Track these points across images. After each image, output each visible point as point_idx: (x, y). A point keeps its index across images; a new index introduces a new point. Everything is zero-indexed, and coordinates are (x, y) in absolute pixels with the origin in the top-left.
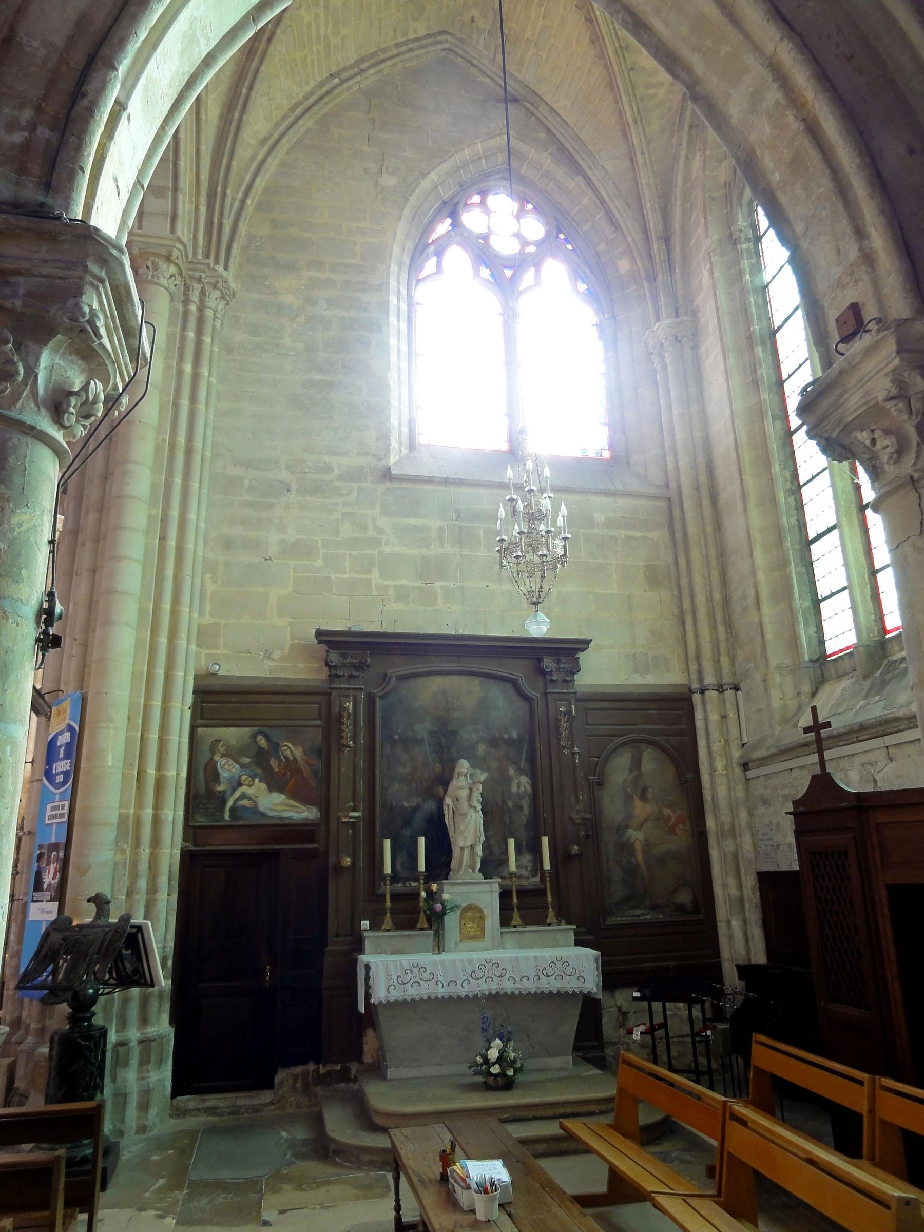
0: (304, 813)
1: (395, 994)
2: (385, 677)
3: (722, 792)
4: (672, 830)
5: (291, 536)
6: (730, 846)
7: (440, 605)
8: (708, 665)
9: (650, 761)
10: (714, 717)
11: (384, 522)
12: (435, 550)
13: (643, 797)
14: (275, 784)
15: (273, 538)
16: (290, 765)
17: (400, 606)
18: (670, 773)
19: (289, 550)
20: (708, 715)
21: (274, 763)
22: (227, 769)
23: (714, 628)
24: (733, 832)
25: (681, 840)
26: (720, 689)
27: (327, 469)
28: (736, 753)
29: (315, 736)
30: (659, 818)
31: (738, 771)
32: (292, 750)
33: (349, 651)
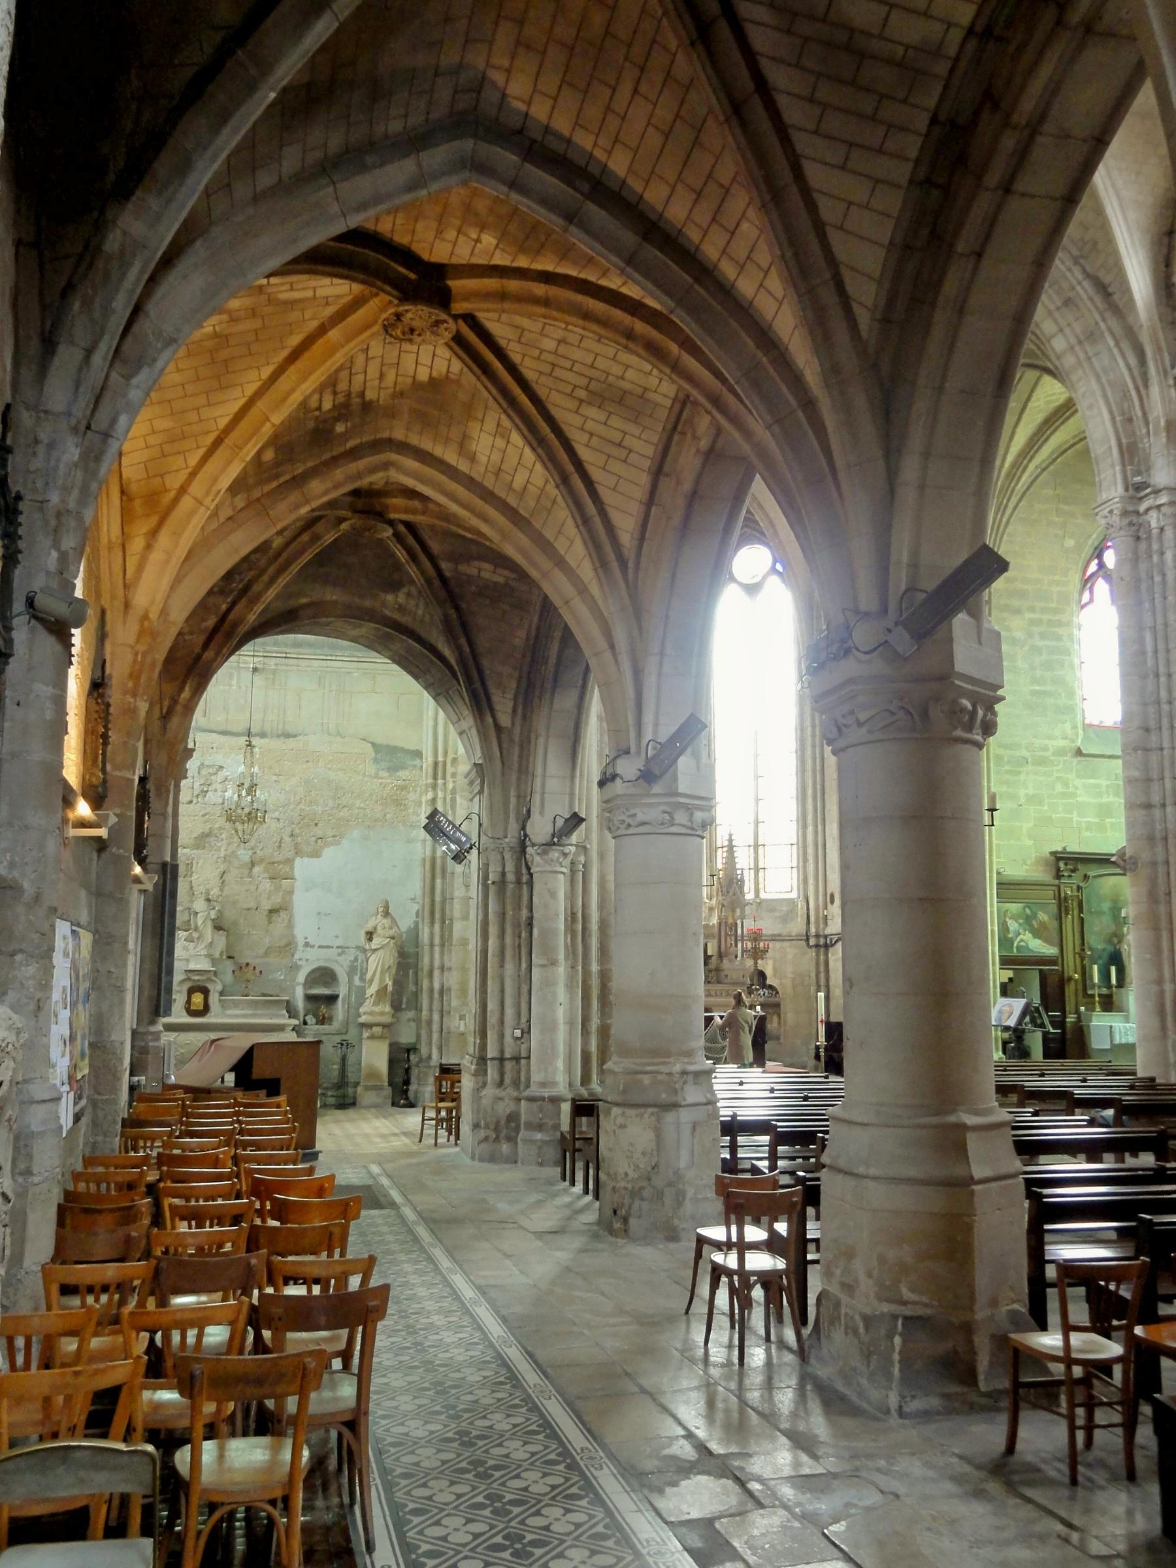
0: (1051, 951)
1: (1124, 1041)
2: (1086, 877)
5: (1031, 791)
7: (1109, 833)
11: (1078, 782)
12: (1105, 800)
14: (1037, 934)
15: (1022, 792)
16: (1042, 924)
17: (1088, 834)
19: (1034, 799)
21: (1034, 923)
22: (1013, 926)
27: (1046, 749)
29: (1054, 909)
32: (1043, 916)
33: (1060, 858)
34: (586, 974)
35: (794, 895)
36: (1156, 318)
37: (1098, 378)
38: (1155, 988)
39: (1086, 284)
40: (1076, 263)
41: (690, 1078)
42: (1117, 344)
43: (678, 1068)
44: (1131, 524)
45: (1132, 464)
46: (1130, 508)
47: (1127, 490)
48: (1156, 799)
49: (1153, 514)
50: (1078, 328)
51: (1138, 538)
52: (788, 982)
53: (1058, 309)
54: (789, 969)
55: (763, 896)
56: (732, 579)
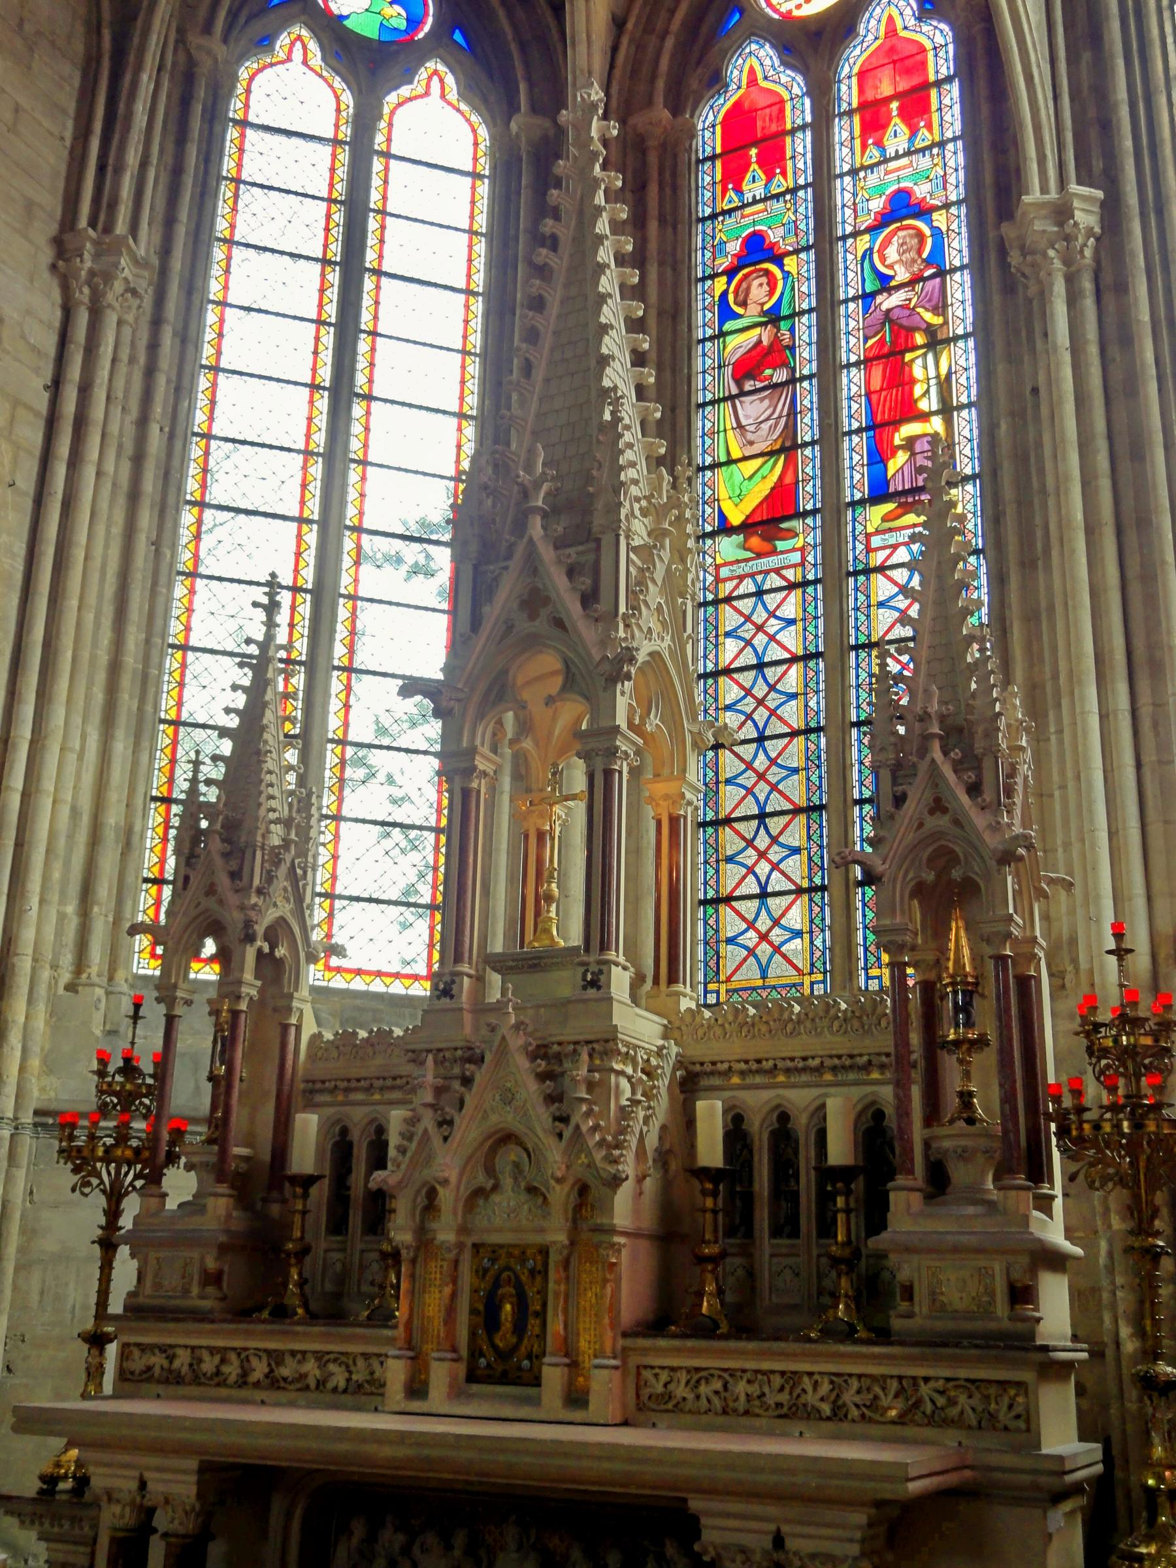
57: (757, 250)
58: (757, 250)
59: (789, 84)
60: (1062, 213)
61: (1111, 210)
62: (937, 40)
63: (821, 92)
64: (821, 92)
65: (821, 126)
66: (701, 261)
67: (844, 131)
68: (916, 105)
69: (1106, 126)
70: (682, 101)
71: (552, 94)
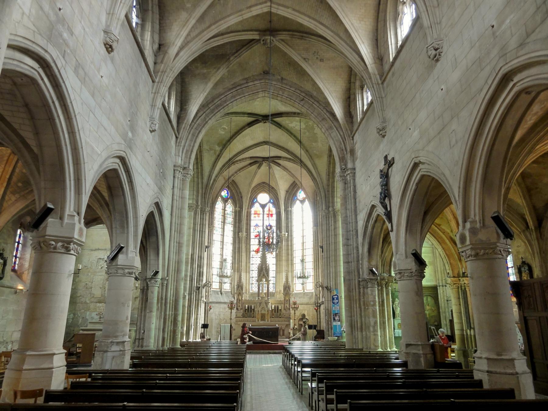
3: (443, 305)
4: (433, 311)
6: (444, 315)
8: (440, 281)
9: (429, 299)
10: (442, 291)
13: (428, 305)
18: (433, 301)
20: (440, 291)
23: (441, 274)
24: (445, 312)
25: (435, 313)
26: (443, 286)
28: (446, 298)
30: (431, 309)
31: (446, 302)
34: (165, 315)
35: (313, 291)
36: (345, 122)
37: (333, 140)
38: (349, 318)
39: (327, 114)
40: (324, 108)
41: (115, 344)
42: (337, 130)
43: (110, 341)
44: (343, 179)
45: (343, 162)
46: (342, 175)
47: (341, 170)
48: (350, 260)
49: (348, 176)
50: (326, 125)
51: (346, 183)
52: (311, 317)
53: (320, 121)
54: (311, 313)
55: (306, 291)
56: (297, 199)
57: (257, 226)
58: (257, 226)
59: (261, 210)
60: (285, 235)
61: (288, 235)
62: (274, 211)
63: (264, 212)
64: (264, 212)
65: (263, 215)
66: (252, 225)
67: (265, 216)
68: (272, 215)
69: (288, 227)
70: (251, 208)
71: (241, 207)
